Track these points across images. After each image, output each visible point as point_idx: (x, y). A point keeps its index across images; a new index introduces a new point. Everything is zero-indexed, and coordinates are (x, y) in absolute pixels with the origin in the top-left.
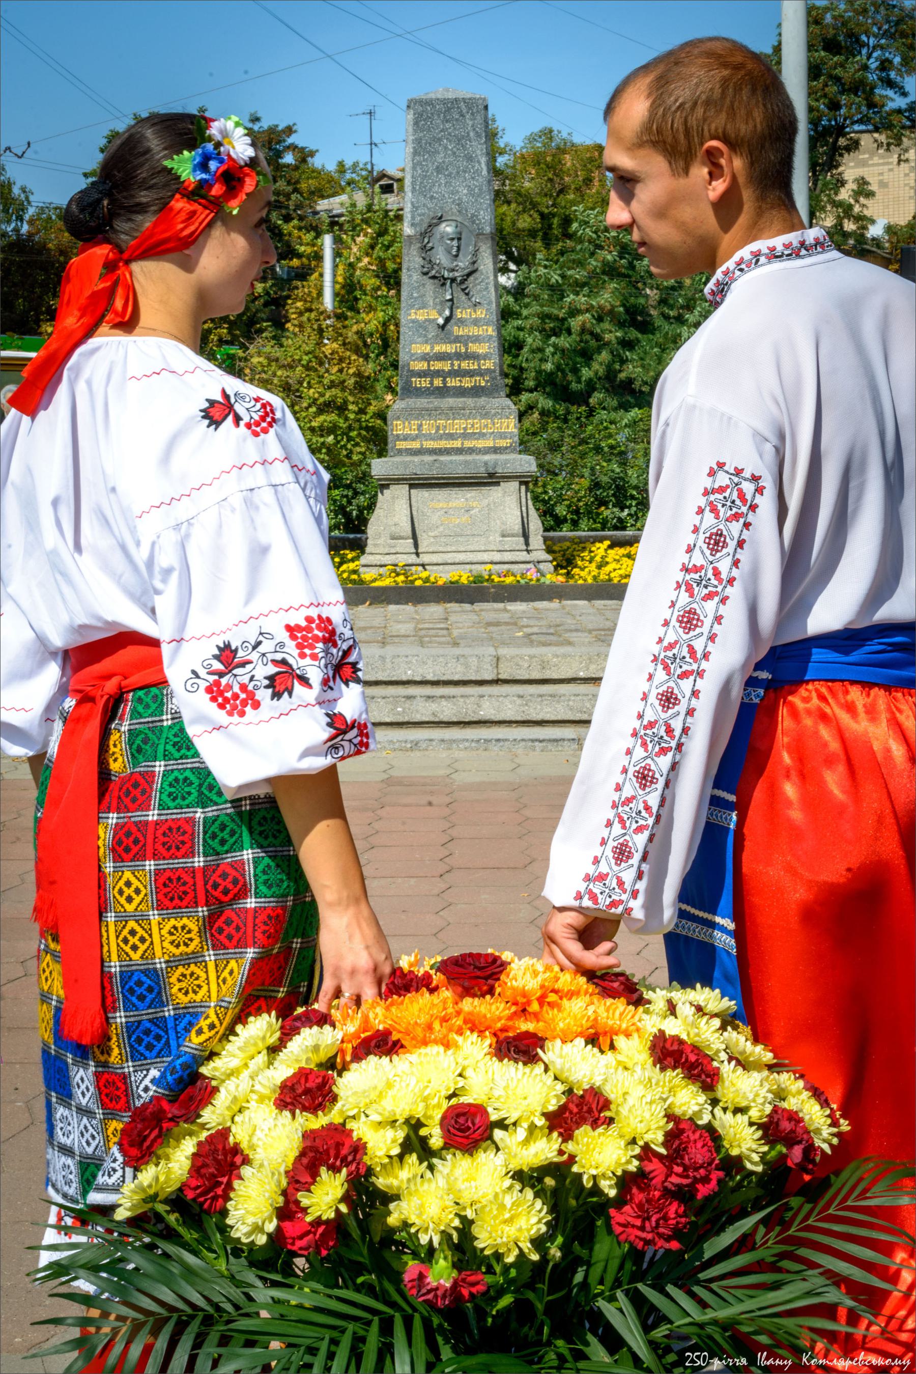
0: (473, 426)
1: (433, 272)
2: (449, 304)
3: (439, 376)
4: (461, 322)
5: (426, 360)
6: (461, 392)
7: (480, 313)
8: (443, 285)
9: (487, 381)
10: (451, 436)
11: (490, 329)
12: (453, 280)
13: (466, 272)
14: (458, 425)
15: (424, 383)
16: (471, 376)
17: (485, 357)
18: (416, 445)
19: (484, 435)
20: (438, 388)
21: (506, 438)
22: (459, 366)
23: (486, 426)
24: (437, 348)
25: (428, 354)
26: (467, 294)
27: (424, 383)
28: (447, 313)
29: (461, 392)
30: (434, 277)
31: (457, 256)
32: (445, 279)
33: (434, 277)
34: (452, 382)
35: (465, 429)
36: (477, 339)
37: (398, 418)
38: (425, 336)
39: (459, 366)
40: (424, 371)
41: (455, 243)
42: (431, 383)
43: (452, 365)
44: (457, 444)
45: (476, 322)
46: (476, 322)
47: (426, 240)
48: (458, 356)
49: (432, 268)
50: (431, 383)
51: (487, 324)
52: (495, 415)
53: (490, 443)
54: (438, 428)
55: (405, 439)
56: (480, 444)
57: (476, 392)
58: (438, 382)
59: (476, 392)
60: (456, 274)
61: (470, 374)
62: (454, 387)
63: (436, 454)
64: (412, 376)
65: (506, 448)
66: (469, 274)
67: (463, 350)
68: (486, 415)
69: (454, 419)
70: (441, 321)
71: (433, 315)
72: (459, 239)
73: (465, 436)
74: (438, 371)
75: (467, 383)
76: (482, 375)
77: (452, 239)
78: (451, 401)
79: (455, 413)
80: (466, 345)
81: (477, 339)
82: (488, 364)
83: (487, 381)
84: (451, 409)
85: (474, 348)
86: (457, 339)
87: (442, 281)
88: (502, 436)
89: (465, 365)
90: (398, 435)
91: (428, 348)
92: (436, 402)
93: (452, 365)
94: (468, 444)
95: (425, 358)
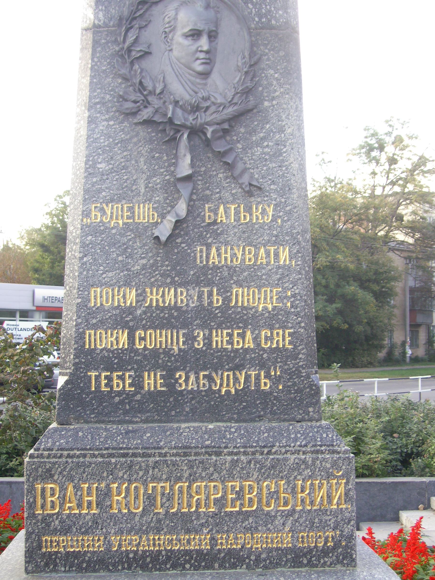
0: (240, 495)
1: (146, 114)
2: (185, 190)
3: (155, 367)
4: (213, 232)
5: (124, 326)
6: (211, 406)
7: (263, 213)
8: (173, 141)
9: (276, 380)
10: (185, 522)
11: (284, 255)
12: (196, 132)
13: (230, 111)
14: (202, 494)
15: (123, 382)
16: (238, 367)
17: (274, 319)
18: (93, 544)
19: (270, 518)
20: (154, 396)
21: (323, 526)
22: (208, 339)
23: (274, 495)
24: (153, 297)
25: (130, 310)
26: (230, 166)
27: (123, 382)
28: (182, 208)
29: (211, 406)
30: (148, 122)
31: (205, 75)
32: (178, 129)
33: (148, 122)
34: (188, 382)
35: (221, 502)
36: (253, 277)
37: (48, 476)
38: (125, 267)
39: (208, 339)
40: (119, 354)
41: (204, 43)
42: (138, 383)
43: (190, 338)
44: (200, 542)
45: (249, 235)
46: (249, 235)
47: (131, 38)
48: (208, 317)
49: (147, 104)
50: (138, 383)
51: (278, 242)
52: (297, 467)
53: (284, 539)
54: (151, 500)
55: (66, 530)
56: (258, 541)
57: (248, 406)
58: (152, 381)
59: (248, 406)
60: (203, 118)
61: (235, 361)
62: (195, 394)
63: (144, 567)
64: (89, 366)
65: (325, 552)
66: (236, 118)
67: (217, 300)
68: (273, 470)
69: (192, 479)
70: (164, 230)
71: (145, 213)
72: (212, 36)
73: (220, 521)
74: (155, 353)
75: (227, 383)
76: (262, 365)
77: (195, 34)
78: (188, 430)
79: (195, 462)
80: (225, 291)
81: (253, 277)
82: (282, 339)
83: (276, 380)
84: (185, 450)
85: (242, 296)
86: (206, 276)
87: (166, 131)
88: (315, 519)
89: (220, 339)
90: (46, 520)
91: (132, 296)
92: (148, 433)
93: (190, 338)
94: (227, 542)
95: (123, 319)
